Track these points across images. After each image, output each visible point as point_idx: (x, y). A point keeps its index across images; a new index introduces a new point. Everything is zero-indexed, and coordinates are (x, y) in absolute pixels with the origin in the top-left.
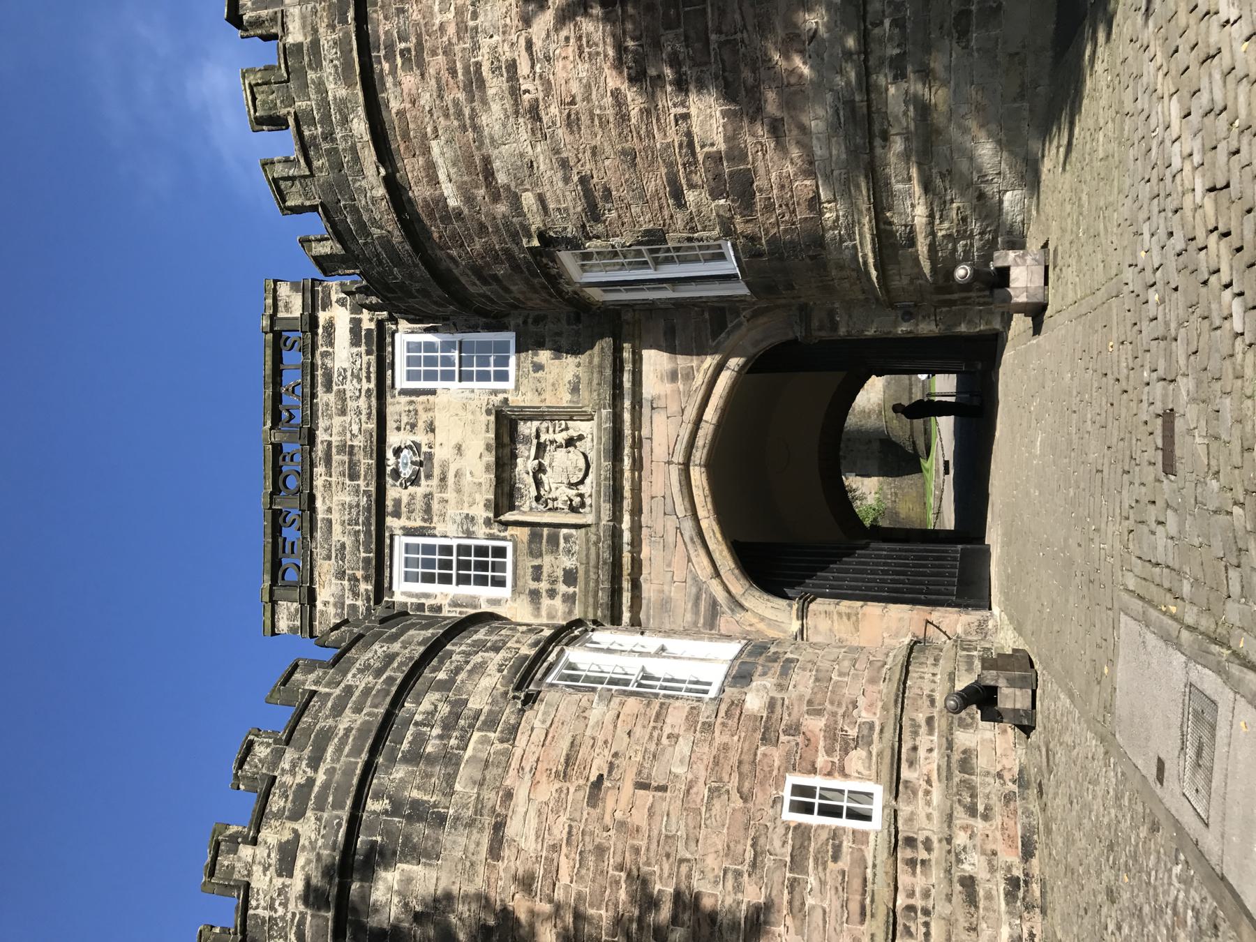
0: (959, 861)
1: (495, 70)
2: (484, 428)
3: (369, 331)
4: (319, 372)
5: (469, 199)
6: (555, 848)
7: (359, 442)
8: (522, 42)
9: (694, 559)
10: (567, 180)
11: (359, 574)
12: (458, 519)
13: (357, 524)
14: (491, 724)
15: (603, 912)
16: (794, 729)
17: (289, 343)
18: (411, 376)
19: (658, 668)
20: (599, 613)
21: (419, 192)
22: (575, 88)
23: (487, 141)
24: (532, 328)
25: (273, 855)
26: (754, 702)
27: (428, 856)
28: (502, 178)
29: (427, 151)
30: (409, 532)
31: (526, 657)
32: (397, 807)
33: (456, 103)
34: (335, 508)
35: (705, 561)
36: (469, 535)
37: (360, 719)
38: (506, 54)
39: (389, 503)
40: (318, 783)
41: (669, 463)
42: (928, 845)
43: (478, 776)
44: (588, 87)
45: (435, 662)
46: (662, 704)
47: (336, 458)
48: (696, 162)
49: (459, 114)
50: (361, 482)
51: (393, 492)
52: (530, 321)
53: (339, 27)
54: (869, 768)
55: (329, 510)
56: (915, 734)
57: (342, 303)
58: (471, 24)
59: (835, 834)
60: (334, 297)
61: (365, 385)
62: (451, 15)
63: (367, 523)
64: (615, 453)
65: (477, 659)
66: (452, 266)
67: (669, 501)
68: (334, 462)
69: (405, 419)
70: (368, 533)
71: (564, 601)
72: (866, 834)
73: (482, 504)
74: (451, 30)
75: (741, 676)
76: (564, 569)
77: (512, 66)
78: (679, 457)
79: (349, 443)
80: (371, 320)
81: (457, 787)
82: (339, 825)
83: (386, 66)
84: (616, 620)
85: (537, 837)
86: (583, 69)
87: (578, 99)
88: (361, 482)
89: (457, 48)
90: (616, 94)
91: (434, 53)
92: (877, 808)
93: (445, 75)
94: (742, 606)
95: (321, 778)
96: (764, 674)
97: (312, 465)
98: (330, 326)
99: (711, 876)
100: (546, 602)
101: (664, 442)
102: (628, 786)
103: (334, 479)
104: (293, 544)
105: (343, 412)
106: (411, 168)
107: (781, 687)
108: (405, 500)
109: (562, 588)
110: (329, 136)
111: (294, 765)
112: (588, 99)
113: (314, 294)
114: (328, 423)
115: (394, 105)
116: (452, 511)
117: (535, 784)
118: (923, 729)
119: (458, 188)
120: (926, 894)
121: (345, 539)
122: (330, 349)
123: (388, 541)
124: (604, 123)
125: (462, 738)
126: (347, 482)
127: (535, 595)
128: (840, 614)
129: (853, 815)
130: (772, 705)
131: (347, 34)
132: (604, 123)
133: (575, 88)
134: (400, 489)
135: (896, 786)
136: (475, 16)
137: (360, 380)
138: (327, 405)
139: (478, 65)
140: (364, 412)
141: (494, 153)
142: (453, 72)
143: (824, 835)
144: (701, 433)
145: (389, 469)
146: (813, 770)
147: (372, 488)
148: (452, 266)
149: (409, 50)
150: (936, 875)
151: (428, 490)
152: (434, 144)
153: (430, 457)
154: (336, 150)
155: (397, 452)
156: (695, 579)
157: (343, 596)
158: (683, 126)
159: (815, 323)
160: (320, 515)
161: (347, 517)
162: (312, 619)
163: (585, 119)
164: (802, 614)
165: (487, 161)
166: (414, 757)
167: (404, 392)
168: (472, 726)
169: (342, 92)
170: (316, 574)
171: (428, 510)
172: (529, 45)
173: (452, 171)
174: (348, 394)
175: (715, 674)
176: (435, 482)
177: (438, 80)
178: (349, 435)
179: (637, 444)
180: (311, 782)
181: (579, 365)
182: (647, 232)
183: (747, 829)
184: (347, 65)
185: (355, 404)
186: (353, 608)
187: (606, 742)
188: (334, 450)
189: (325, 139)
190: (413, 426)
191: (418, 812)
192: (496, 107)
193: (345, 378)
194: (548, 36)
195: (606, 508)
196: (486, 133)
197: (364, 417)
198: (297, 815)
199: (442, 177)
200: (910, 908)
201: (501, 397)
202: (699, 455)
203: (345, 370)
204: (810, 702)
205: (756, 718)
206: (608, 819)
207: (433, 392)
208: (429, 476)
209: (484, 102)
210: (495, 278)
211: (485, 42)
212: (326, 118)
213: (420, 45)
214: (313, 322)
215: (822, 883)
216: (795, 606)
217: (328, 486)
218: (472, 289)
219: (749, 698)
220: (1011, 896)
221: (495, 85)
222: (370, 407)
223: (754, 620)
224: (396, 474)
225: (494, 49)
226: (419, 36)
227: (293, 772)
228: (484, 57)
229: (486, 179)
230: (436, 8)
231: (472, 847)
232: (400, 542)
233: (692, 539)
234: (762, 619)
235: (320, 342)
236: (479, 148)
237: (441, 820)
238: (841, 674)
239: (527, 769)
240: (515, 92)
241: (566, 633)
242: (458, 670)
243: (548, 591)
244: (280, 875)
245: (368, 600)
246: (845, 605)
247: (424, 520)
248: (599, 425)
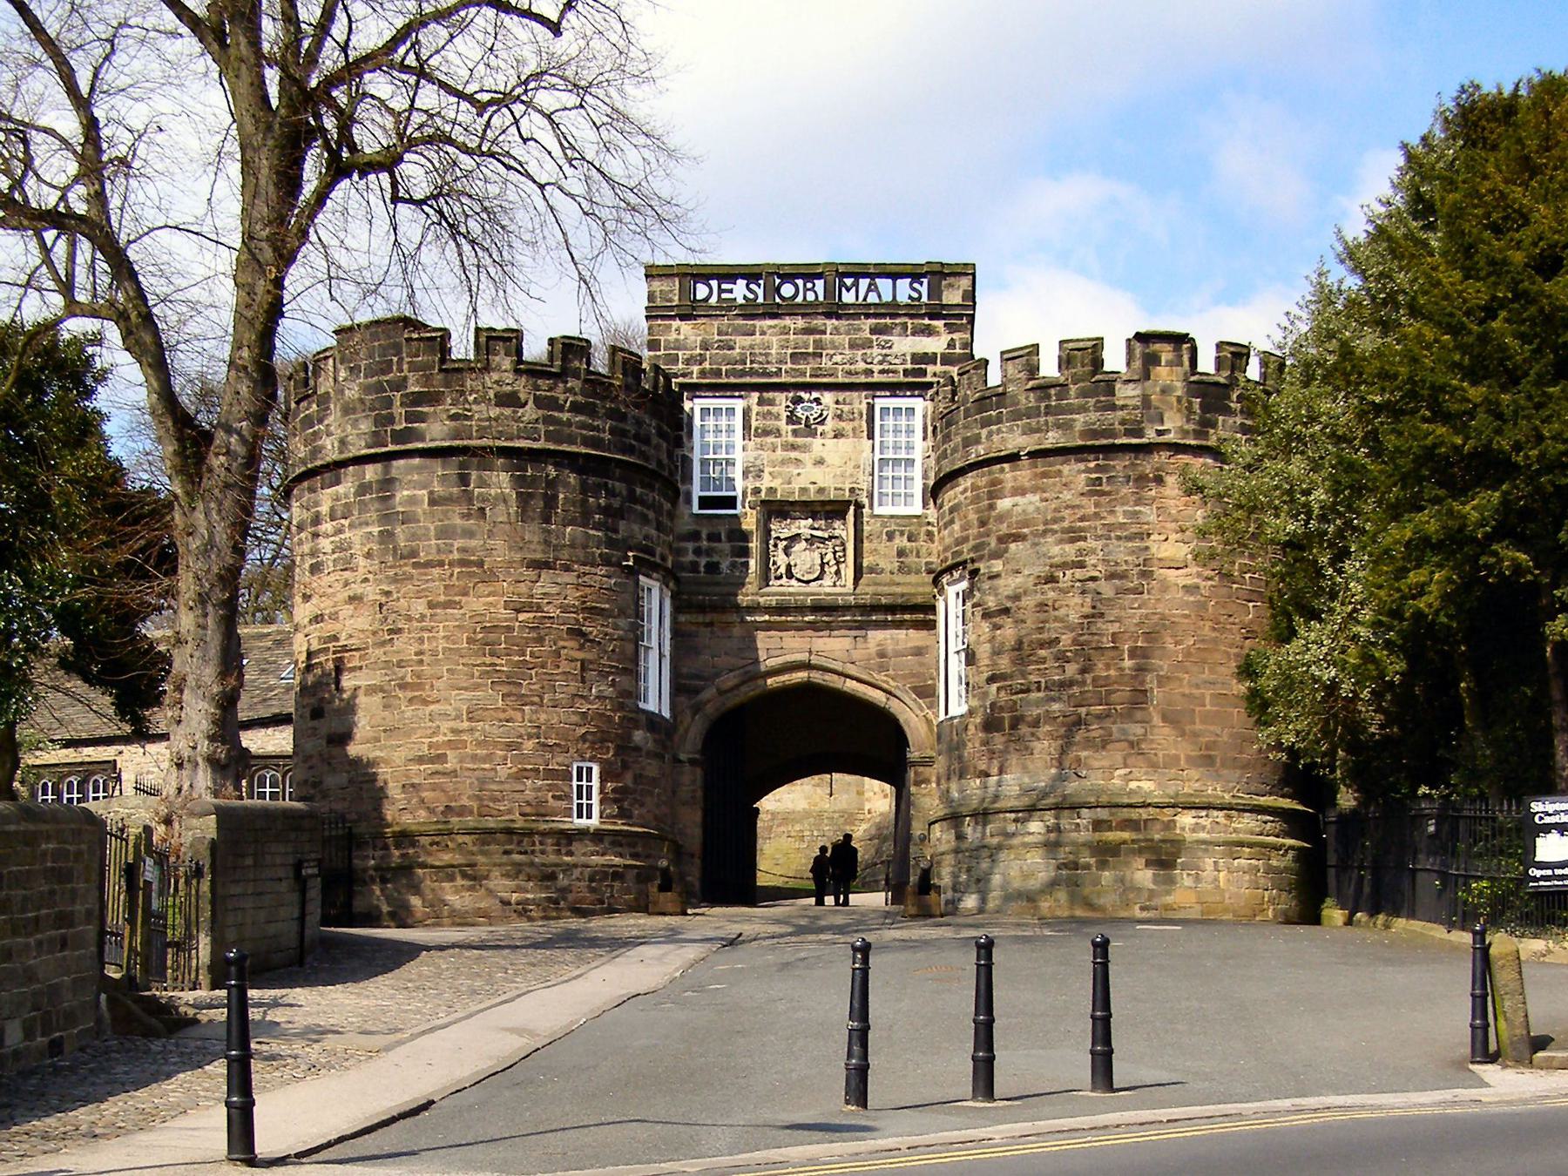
0: (564, 871)
1: (1080, 552)
2: (839, 486)
3: (924, 373)
4: (888, 321)
5: (1001, 518)
6: (539, 609)
7: (826, 363)
8: (1097, 574)
9: (731, 674)
10: (1008, 597)
11: (707, 365)
12: (758, 462)
13: (752, 362)
14: (611, 543)
15: (503, 646)
16: (625, 766)
17: (916, 285)
18: (884, 410)
19: (653, 656)
20: (685, 597)
21: (1007, 474)
22: (1062, 612)
23: (1036, 540)
24: (924, 529)
25: (509, 388)
26: (639, 736)
27: (524, 511)
28: (1013, 546)
29: (1034, 490)
30: (746, 413)
31: (653, 555)
32: (552, 484)
33: (1063, 519)
34: (766, 338)
35: (730, 684)
36: (745, 474)
37: (607, 436)
38: (1091, 560)
39: (770, 395)
40: (561, 415)
41: (810, 652)
42: (570, 854)
43: (578, 541)
44: (1062, 621)
45: (647, 480)
46: (631, 671)
47: (812, 338)
48: (1012, 694)
49: (1055, 521)
50: (789, 365)
51: (782, 399)
52: (930, 528)
53: (1122, 428)
54: (607, 817)
55: (763, 333)
56: (630, 845)
57: (951, 345)
58: (1112, 535)
59: (568, 797)
60: (956, 336)
61: (876, 368)
62: (1121, 520)
63: (752, 373)
64: (817, 608)
65: (651, 515)
66: (960, 489)
67: (779, 652)
68: (806, 337)
69: (846, 408)
70: (743, 373)
71: (691, 562)
72: (570, 816)
73: (773, 485)
74: (1110, 520)
75: (653, 721)
76: (718, 563)
77: (1081, 565)
78: (815, 660)
79: (824, 353)
80: (935, 375)
81: (569, 529)
82: (535, 440)
83: (1092, 465)
84: (677, 610)
85: (544, 594)
86: (1074, 618)
87: (1056, 613)
88: (789, 365)
89: (1098, 523)
90: (1057, 641)
91: (1096, 505)
92: (583, 822)
93: (1080, 513)
94: (695, 714)
95: (565, 416)
96: (655, 741)
97: (804, 315)
98: (929, 332)
99: (534, 717)
100: (690, 546)
101: (828, 648)
102: (580, 655)
103: (792, 337)
104: (731, 291)
105: (853, 346)
106: (1023, 474)
107: (649, 754)
108: (774, 409)
109: (703, 561)
110: (1049, 411)
111: (571, 390)
112: (1056, 619)
113: (960, 316)
114: (842, 330)
115: (1066, 469)
116: (765, 454)
117: (577, 587)
118: (632, 850)
119: (1008, 511)
120: (543, 852)
121: (738, 350)
122: (909, 332)
123: (737, 394)
124: (1040, 630)
125: (599, 523)
126: (790, 351)
127: (695, 536)
128: (694, 791)
129: (580, 806)
130: (637, 749)
131: (1113, 435)
132: (1040, 630)
133: (1062, 612)
134: (784, 405)
135: (597, 836)
136: (1119, 538)
137: (881, 363)
138: (860, 329)
139: (1085, 539)
140: (852, 367)
141: (1027, 544)
142: (1082, 519)
143: (566, 789)
144: (836, 677)
145: (802, 394)
146: (603, 780)
147: (783, 379)
148: (960, 489)
149: (1100, 485)
150: (552, 858)
151: (784, 433)
152: (1037, 497)
153: (813, 434)
154: (1039, 415)
155: (817, 401)
156: (717, 675)
157: (686, 349)
158: (1034, 687)
159: (921, 769)
160: (758, 323)
161: (757, 351)
162: (663, 317)
163: (1042, 616)
164: (692, 762)
165: (1022, 538)
166: (584, 489)
167: (871, 408)
168: (608, 529)
169: (1078, 427)
170: (703, 320)
171: (766, 433)
172: (1093, 579)
173: (1019, 509)
174: (869, 351)
175: (651, 706)
176: (791, 439)
177: (1078, 507)
178: (832, 352)
179: (829, 627)
180: (561, 409)
181: (892, 573)
182: (974, 653)
183: (566, 740)
184: (1095, 434)
185: (859, 358)
186: (675, 360)
187: (606, 634)
188: (818, 337)
189: (1047, 407)
190: (840, 417)
191: (550, 502)
192: (1056, 550)
193: (883, 347)
194: (1099, 593)
195: (773, 601)
196: (1042, 541)
197: (847, 367)
198: (539, 402)
199: (1018, 499)
200: (534, 844)
201: (866, 501)
202: (817, 677)
203: (890, 347)
204: (641, 775)
205: (629, 737)
206: (561, 643)
207: (871, 436)
208: (795, 433)
209: (1061, 541)
210: (952, 522)
211: (1098, 544)
212: (1060, 410)
213: (1103, 493)
214: (933, 316)
215: (539, 789)
216: (697, 756)
217: (785, 331)
218: (947, 496)
219: (641, 732)
220: (549, 899)
221: (1070, 550)
222: (857, 373)
223: (685, 725)
224: (798, 401)
225: (1093, 551)
226: (1108, 494)
227: (567, 390)
228: (1091, 543)
229: (1013, 535)
230: (1126, 508)
231: (533, 547)
232: (739, 405)
233: (746, 673)
234: (687, 731)
235: (916, 321)
236: (1032, 532)
237: (547, 520)
238: (658, 795)
239: (585, 579)
240: (1064, 566)
241: (670, 576)
242: (643, 503)
243: (699, 547)
244: (496, 395)
245: (684, 375)
246: (699, 794)
247: (756, 429)
248: (840, 594)
